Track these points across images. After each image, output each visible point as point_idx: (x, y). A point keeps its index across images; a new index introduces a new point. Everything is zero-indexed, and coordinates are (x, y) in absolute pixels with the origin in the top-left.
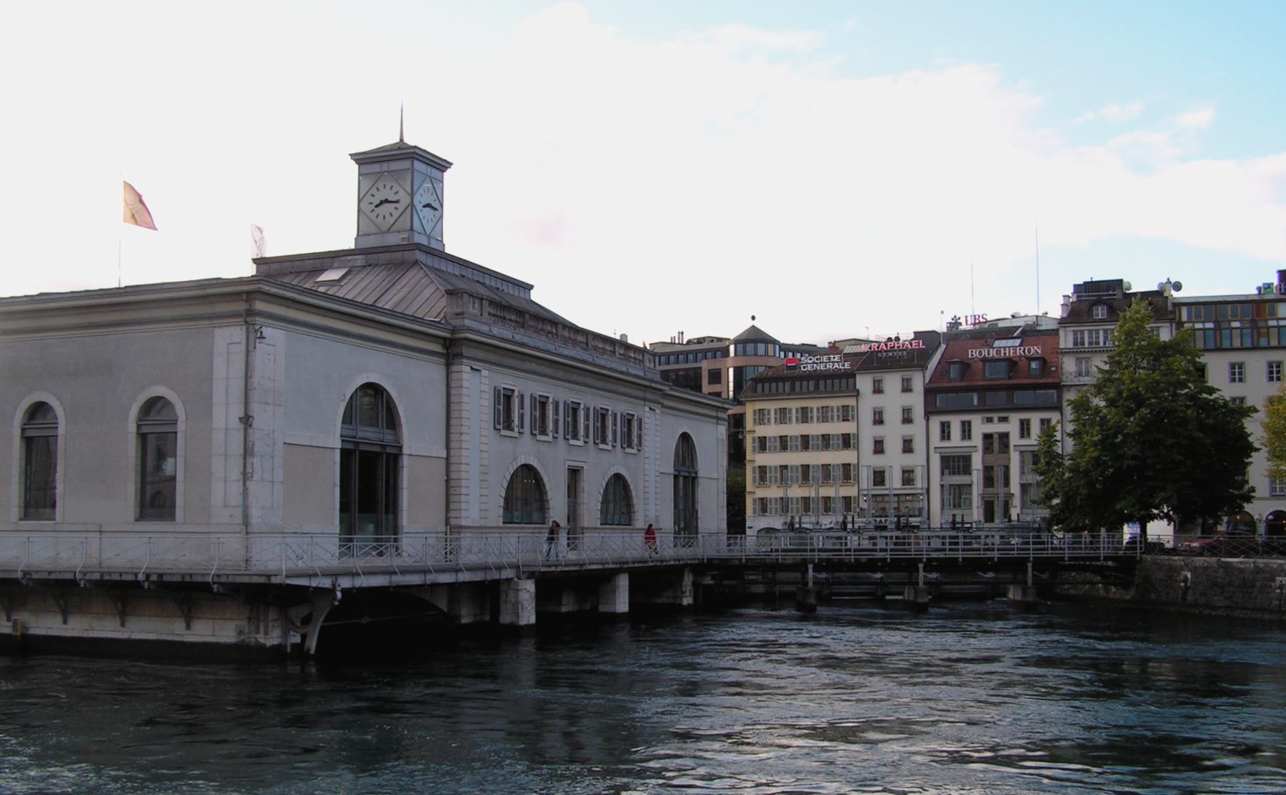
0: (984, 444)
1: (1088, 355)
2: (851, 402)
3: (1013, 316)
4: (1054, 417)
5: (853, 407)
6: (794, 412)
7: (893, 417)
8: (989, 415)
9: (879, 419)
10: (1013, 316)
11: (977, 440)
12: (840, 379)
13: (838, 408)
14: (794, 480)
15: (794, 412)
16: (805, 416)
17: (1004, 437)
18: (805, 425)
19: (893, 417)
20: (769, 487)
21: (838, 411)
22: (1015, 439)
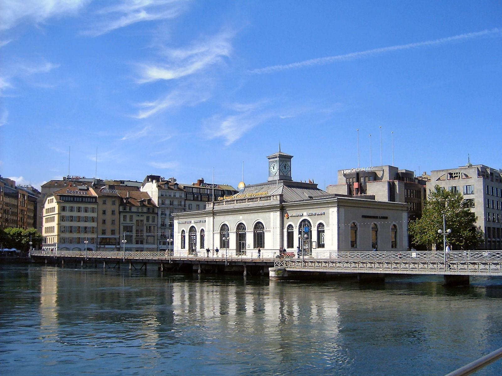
0: (136, 223)
1: (164, 199)
2: (95, 206)
3: (83, 178)
4: (156, 216)
5: (96, 208)
6: (75, 208)
7: (109, 212)
8: (138, 214)
9: (104, 212)
10: (83, 178)
11: (134, 222)
12: (68, 197)
13: (91, 208)
14: (67, 231)
15: (75, 208)
16: (79, 210)
17: (142, 221)
18: (79, 213)
19: (109, 212)
20: (65, 233)
21: (91, 209)
22: (145, 222)
